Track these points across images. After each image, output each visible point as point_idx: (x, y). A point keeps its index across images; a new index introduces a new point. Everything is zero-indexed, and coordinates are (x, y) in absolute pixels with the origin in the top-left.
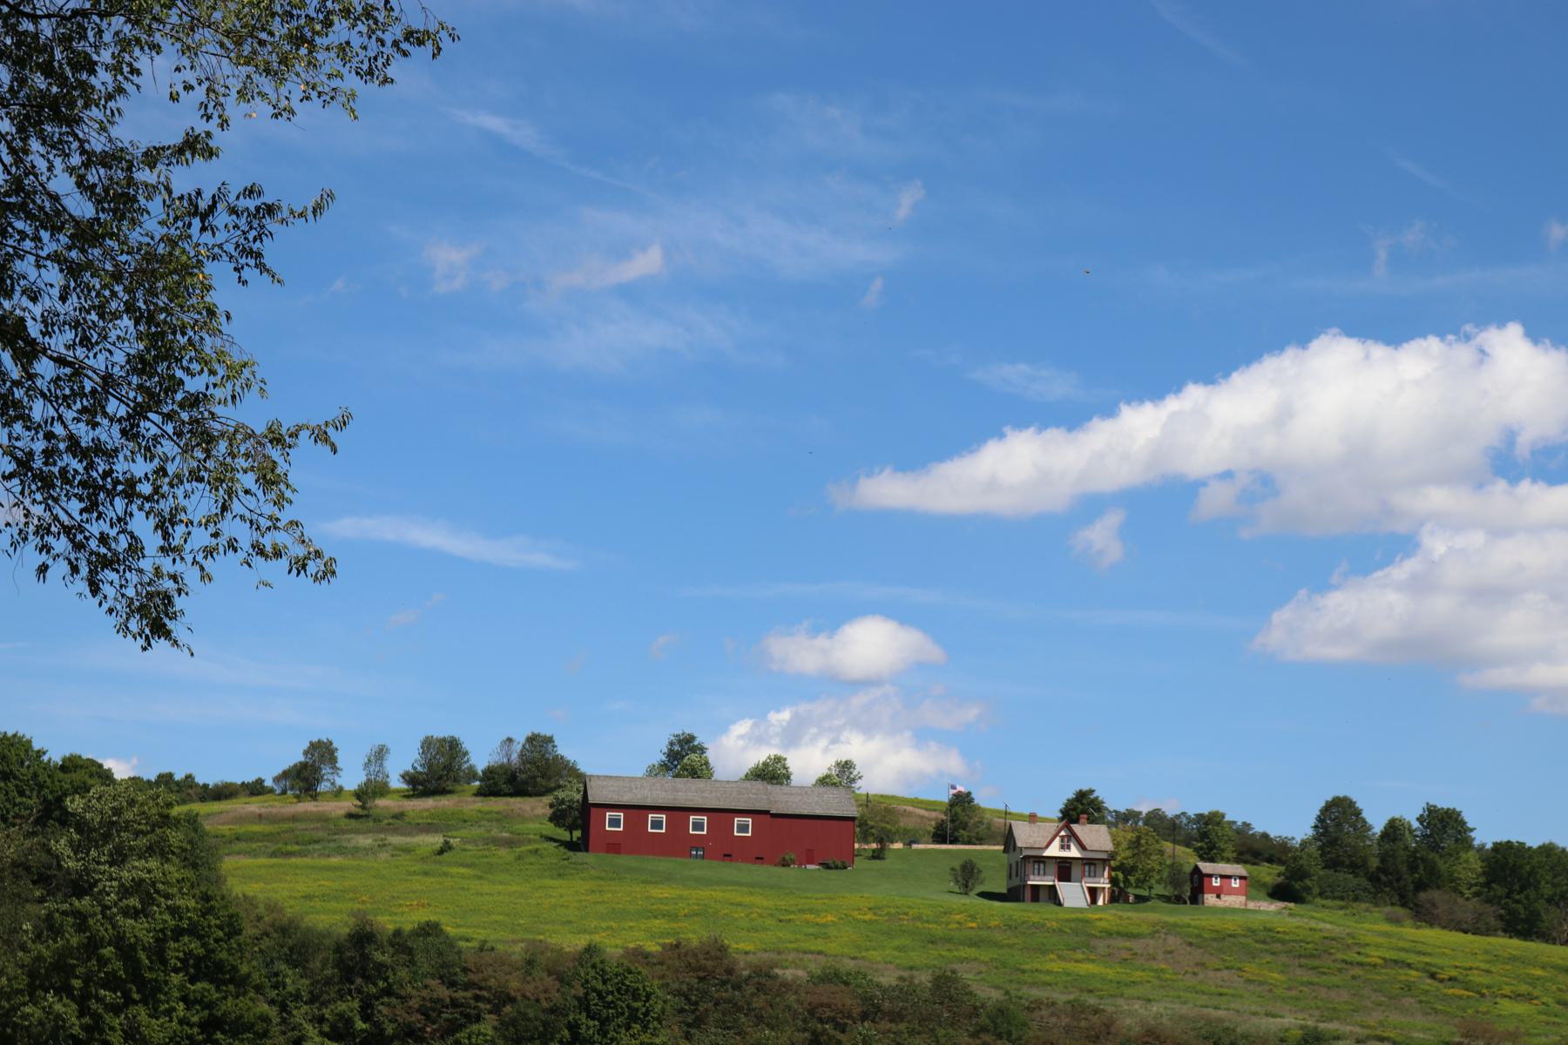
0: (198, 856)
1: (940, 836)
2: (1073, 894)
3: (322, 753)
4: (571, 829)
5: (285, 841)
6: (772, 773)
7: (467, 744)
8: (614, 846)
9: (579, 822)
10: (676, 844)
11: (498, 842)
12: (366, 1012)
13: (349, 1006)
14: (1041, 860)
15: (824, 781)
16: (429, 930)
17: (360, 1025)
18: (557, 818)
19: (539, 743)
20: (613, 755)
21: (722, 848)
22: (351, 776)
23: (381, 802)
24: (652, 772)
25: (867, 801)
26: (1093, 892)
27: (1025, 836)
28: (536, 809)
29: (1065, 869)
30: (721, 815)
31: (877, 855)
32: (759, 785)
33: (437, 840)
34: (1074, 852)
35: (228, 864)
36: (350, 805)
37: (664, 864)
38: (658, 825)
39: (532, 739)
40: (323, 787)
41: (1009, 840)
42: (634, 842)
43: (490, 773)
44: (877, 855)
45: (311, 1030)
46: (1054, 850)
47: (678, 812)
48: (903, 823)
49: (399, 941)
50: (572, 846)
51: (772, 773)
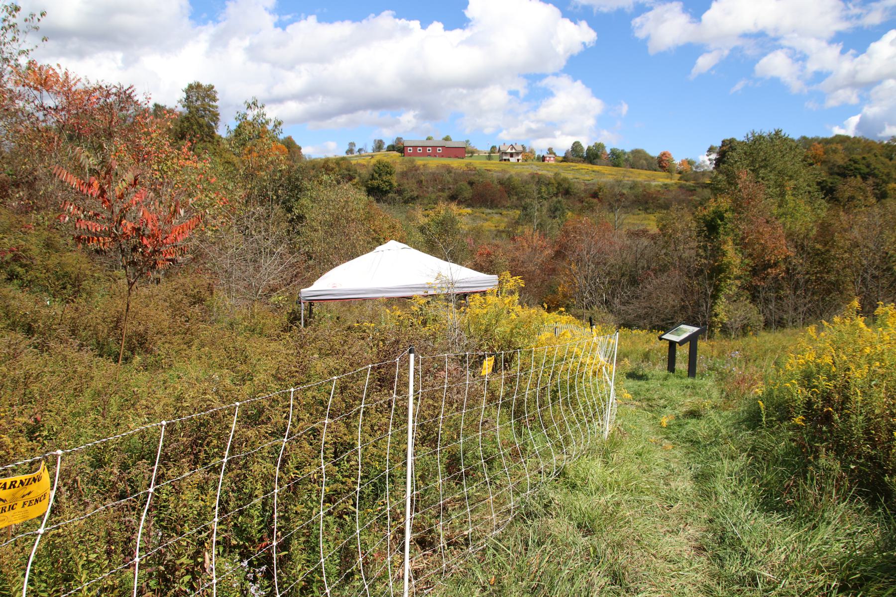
29: (512, 155)
34: (514, 151)
46: (509, 151)
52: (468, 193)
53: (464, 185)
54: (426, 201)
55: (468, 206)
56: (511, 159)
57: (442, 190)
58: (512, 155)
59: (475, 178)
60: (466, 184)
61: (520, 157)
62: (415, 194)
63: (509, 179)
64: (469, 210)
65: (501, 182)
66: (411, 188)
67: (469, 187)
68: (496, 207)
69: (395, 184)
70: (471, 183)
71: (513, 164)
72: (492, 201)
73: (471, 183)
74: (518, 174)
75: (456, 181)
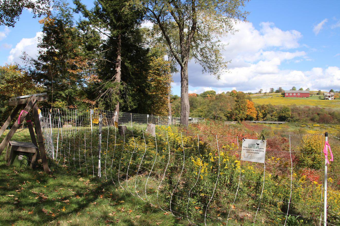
0: (250, 99)
1: (317, 94)
2: (330, 99)
3: (261, 90)
4: (283, 95)
5: (258, 97)
6: (301, 89)
7: (274, 88)
8: (287, 96)
9: (284, 94)
10: (293, 96)
11: (277, 97)
12: (265, 111)
13: (263, 111)
14: (327, 96)
15: (306, 90)
16: (270, 104)
17: (264, 112)
18: (281, 94)
19: (280, 88)
20: (287, 88)
21: (297, 96)
22: (263, 92)
23: (267, 94)
24: (291, 90)
25: (311, 92)
26: (332, 99)
27: (325, 94)
28: (280, 93)
29: (329, 97)
30: (297, 93)
31: (311, 96)
32: (300, 91)
33: (271, 97)
34: (330, 95)
35: (253, 99)
36: (264, 94)
37: (292, 98)
38: (291, 94)
39: (280, 88)
40: (262, 93)
41: (324, 94)
42: (289, 96)
43: (276, 91)
44: (311, 96)
45: (260, 113)
46: (328, 95)
47: (293, 93)
48: (314, 93)
49: (267, 106)
50: (283, 97)
51: (301, 89)
52: (317, 118)
53: (316, 115)
54: (302, 121)
55: (318, 123)
56: (329, 98)
57: (307, 116)
58: (329, 97)
59: (320, 112)
60: (316, 114)
61: (333, 97)
62: (298, 118)
63: (333, 113)
64: (318, 125)
65: (330, 114)
66: (295, 114)
67: (318, 116)
68: (329, 123)
69: (291, 115)
70: (318, 114)
71: (331, 102)
72: (327, 121)
73: (318, 114)
74: (336, 110)
75: (313, 114)
